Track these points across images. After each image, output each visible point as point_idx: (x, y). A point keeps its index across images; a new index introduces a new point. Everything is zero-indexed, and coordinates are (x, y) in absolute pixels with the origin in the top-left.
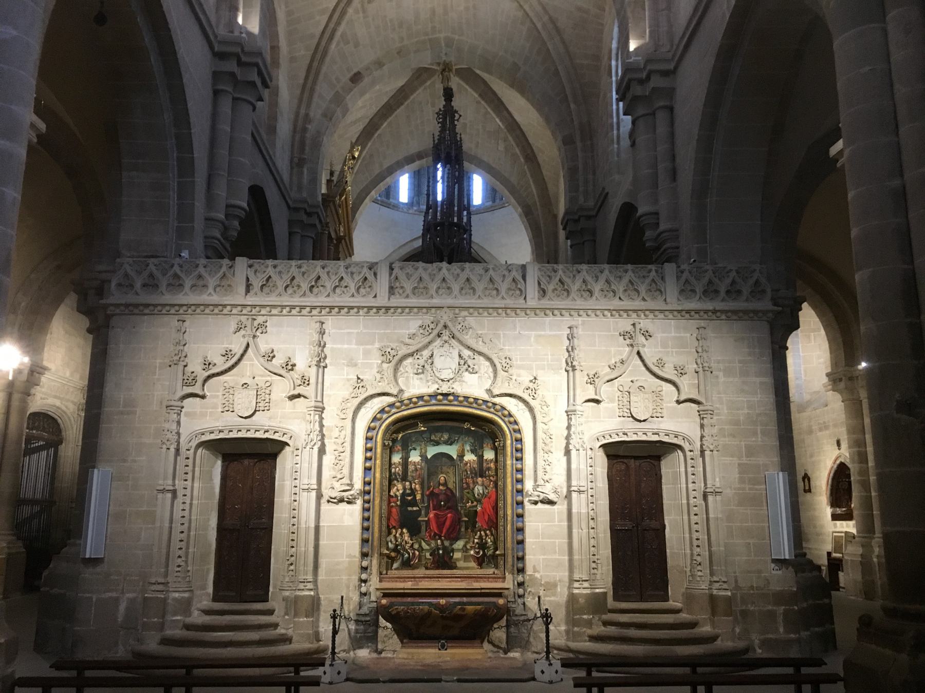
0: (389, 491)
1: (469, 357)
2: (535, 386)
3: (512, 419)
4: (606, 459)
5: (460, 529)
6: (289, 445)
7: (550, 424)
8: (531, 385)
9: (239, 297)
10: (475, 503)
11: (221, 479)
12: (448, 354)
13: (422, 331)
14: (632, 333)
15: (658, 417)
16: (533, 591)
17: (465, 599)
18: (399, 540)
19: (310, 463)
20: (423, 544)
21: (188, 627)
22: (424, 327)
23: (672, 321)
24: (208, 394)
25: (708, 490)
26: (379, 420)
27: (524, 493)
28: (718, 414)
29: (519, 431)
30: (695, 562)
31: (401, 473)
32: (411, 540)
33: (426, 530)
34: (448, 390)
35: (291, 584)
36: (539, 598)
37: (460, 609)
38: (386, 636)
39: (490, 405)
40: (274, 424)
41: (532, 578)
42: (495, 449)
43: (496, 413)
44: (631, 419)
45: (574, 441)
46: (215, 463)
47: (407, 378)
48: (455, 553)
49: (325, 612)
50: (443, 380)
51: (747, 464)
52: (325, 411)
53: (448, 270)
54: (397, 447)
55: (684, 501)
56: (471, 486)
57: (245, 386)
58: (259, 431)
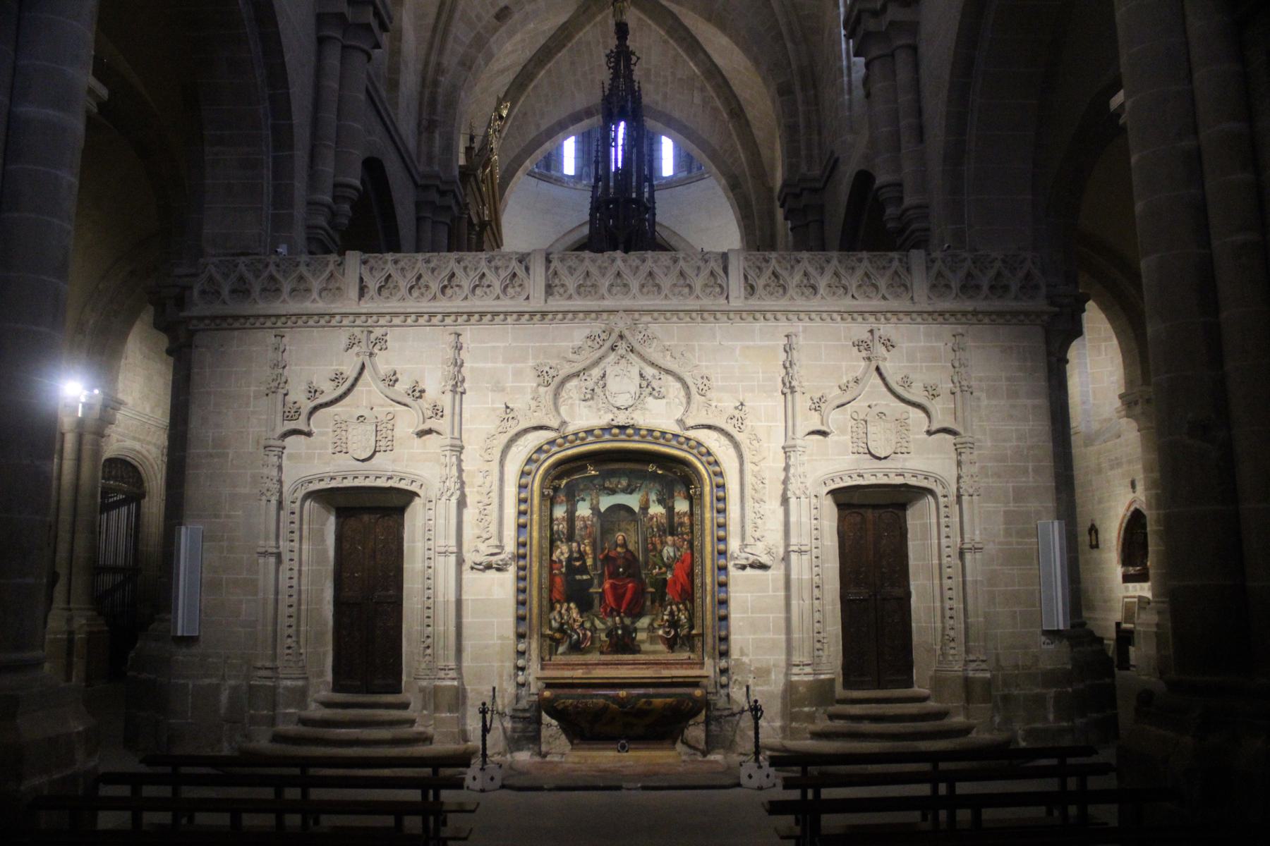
0: (551, 555)
1: (654, 376)
2: (742, 414)
3: (711, 459)
4: (835, 510)
5: (644, 603)
6: (418, 495)
7: (762, 464)
8: (736, 413)
9: (350, 303)
10: (664, 569)
11: (336, 539)
12: (625, 372)
13: (590, 343)
14: (869, 343)
15: (902, 453)
16: (740, 679)
17: (651, 691)
18: (565, 617)
19: (447, 519)
20: (597, 622)
21: (304, 722)
22: (592, 338)
23: (922, 326)
24: (314, 430)
25: (965, 546)
26: (536, 461)
27: (728, 556)
28: (980, 448)
29: (721, 474)
30: (947, 637)
31: (565, 531)
32: (581, 617)
34: (627, 421)
35: (428, 672)
36: (748, 687)
37: (646, 702)
38: (551, 736)
39: (682, 440)
40: (398, 469)
41: (739, 664)
42: (690, 499)
43: (691, 451)
44: (868, 456)
45: (794, 486)
46: (328, 519)
47: (572, 405)
48: (638, 634)
49: (473, 706)
50: (619, 408)
51: (1014, 511)
52: (464, 451)
53: (624, 261)
54: (559, 497)
55: (936, 562)
56: (659, 547)
57: (361, 419)
58: (380, 477)
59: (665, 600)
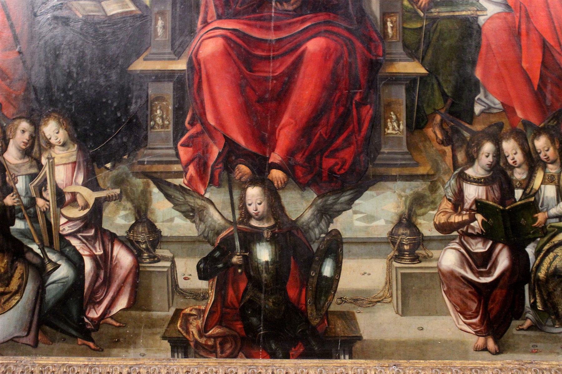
18: (21, 185)
33: (179, 130)
48: (347, 264)
59: (470, 117)
